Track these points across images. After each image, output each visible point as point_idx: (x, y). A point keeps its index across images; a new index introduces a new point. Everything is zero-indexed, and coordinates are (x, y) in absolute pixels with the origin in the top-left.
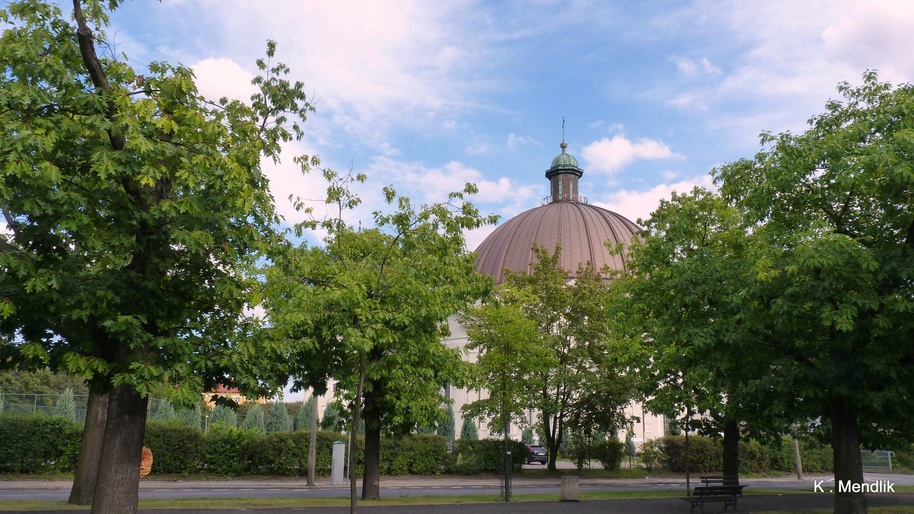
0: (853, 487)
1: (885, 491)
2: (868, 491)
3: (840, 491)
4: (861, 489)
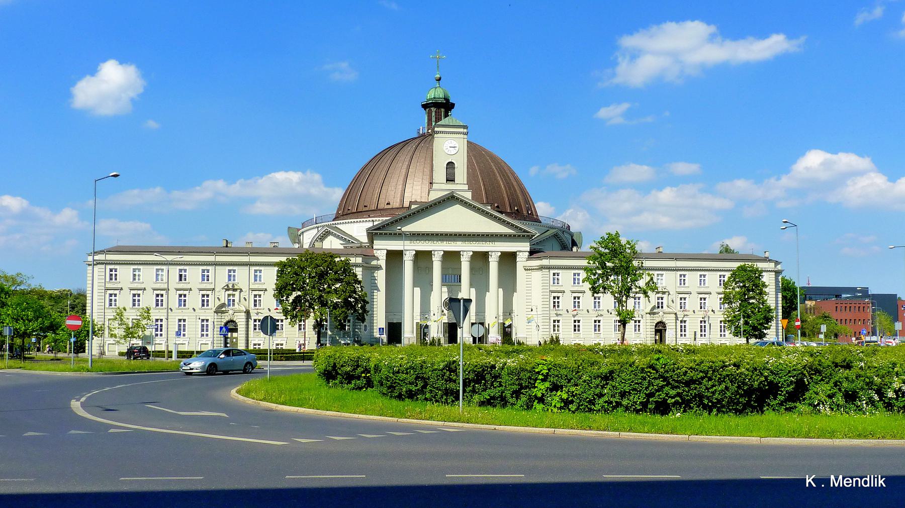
0: (845, 482)
1: (876, 486)
2: (859, 486)
3: (832, 485)
4: (852, 483)
